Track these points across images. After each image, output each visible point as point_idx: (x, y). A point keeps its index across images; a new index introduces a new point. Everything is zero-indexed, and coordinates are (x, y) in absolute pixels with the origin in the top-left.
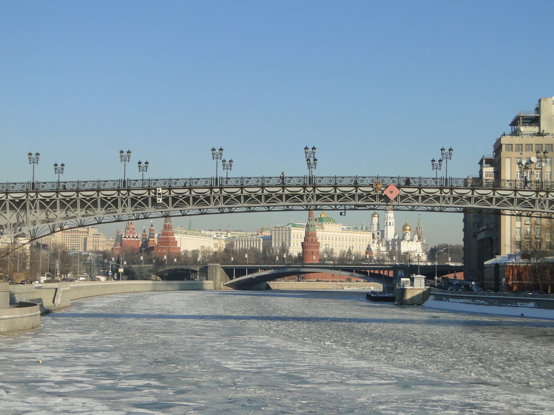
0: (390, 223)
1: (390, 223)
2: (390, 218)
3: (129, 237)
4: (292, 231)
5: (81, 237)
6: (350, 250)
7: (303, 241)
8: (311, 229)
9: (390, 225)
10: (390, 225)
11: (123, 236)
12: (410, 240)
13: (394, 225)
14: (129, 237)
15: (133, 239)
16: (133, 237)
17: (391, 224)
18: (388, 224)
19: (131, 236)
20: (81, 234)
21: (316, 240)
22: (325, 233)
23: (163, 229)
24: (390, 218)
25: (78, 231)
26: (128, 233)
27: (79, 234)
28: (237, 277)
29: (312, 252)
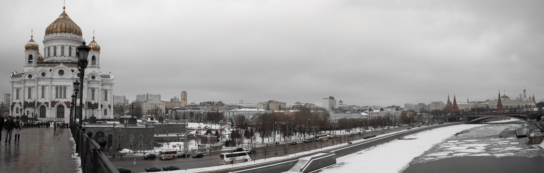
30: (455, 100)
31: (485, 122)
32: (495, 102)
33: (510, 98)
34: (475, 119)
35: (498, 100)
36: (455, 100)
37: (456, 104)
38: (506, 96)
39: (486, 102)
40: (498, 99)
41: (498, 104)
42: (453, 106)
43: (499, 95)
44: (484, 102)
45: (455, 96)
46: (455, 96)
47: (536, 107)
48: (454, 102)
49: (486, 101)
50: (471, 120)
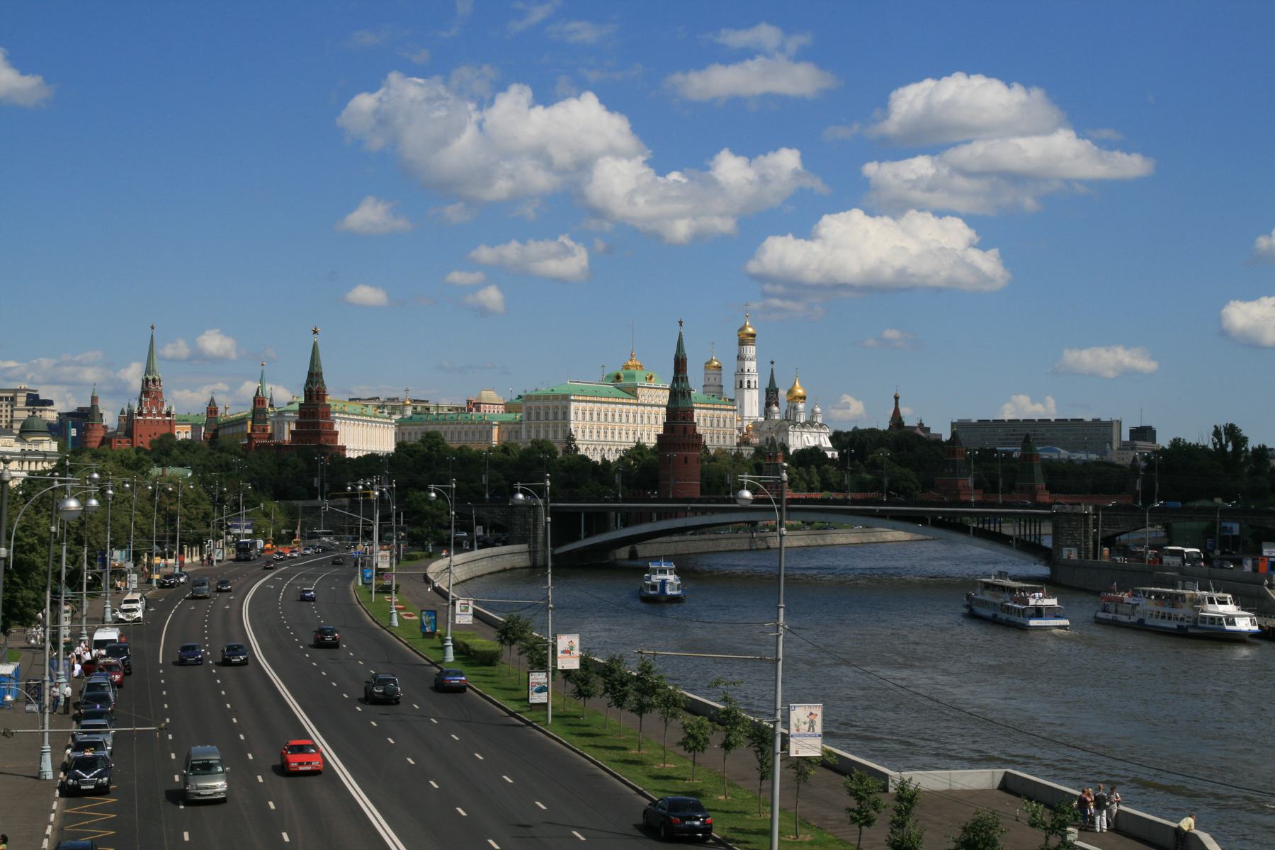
0: (749, 382)
1: (749, 382)
2: (748, 370)
3: (150, 413)
4: (573, 406)
8: (682, 403)
9: (749, 387)
10: (749, 387)
11: (136, 411)
12: (807, 422)
13: (757, 387)
14: (150, 413)
16: (159, 414)
17: (752, 385)
18: (746, 385)
19: (154, 411)
24: (748, 370)
26: (146, 405)
28: (587, 536)
29: (686, 458)
45: (315, 345)
46: (315, 345)
50: (578, 539)
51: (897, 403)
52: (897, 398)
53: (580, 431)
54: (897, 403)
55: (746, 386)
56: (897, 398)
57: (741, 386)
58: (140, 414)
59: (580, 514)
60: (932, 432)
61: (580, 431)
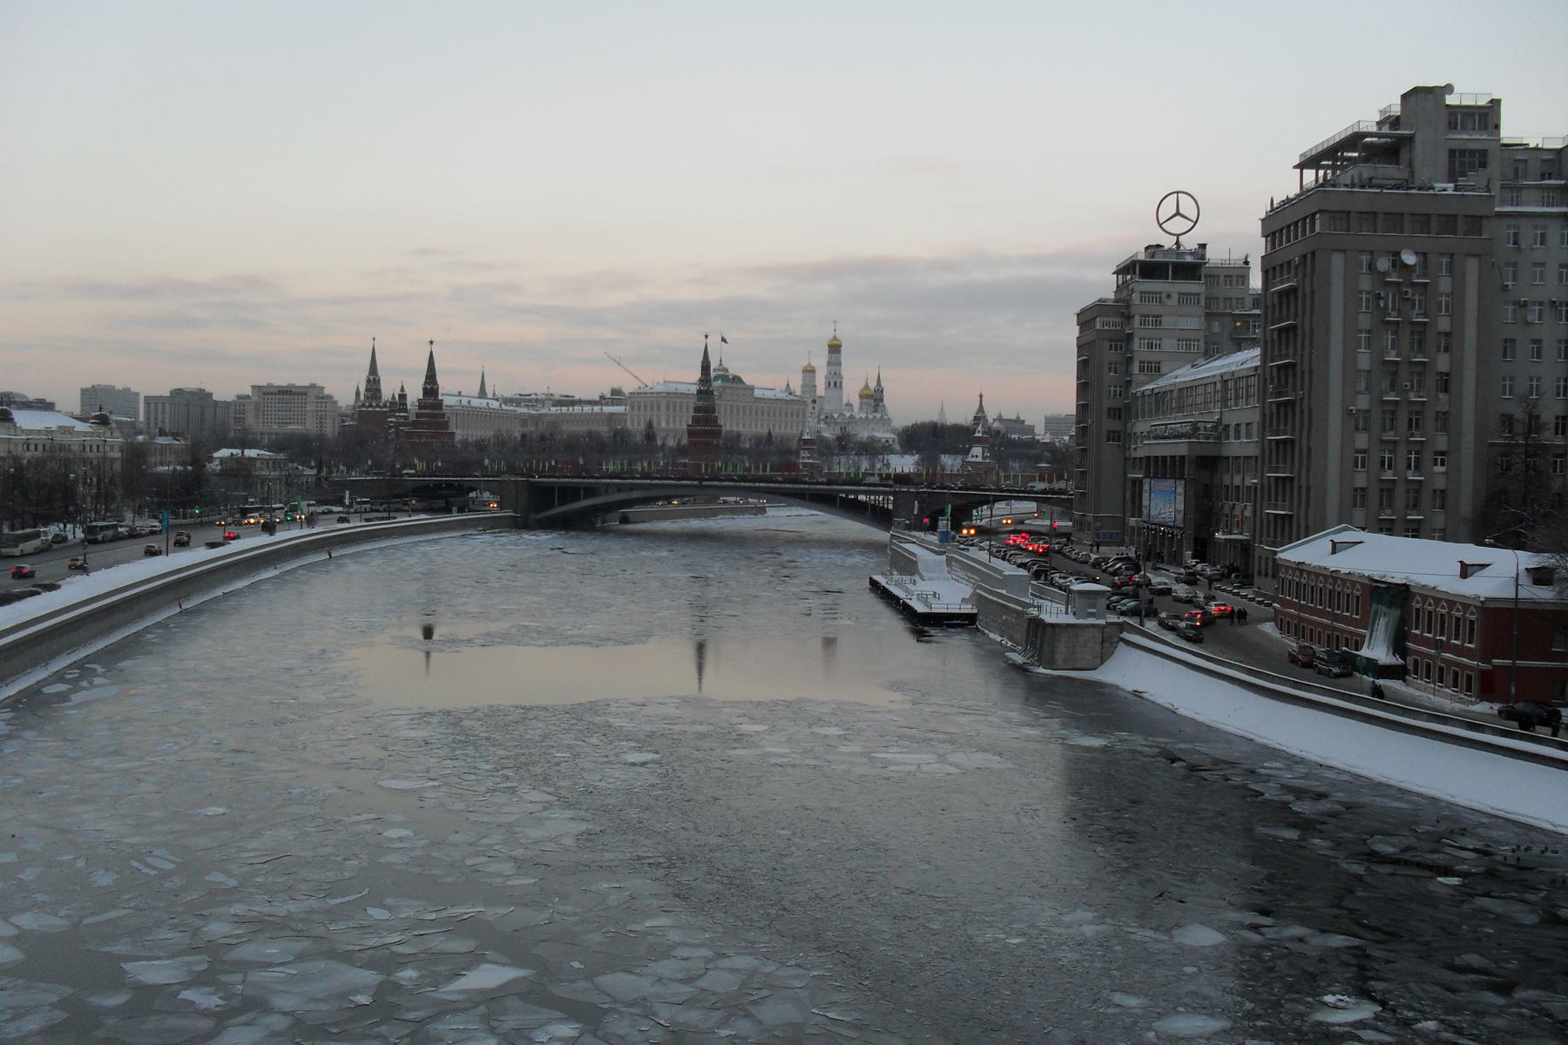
0: (835, 383)
1: (835, 383)
5: (296, 401)
6: (770, 433)
7: (690, 423)
14: (370, 406)
15: (378, 409)
16: (378, 406)
17: (838, 385)
19: (374, 404)
20: (296, 397)
21: (716, 421)
22: (723, 403)
23: (421, 397)
25: (291, 391)
27: (292, 397)
28: (559, 505)
30: (431, 376)
31: (625, 520)
32: (663, 408)
33: (752, 388)
34: (576, 498)
35: (699, 392)
36: (431, 376)
37: (439, 405)
38: (732, 372)
39: (602, 400)
40: (694, 389)
41: (696, 420)
42: (418, 415)
43: (706, 367)
44: (590, 403)
45: (431, 353)
46: (431, 353)
47: (897, 447)
48: (426, 391)
49: (602, 397)
51: (981, 401)
52: (981, 396)
53: (663, 418)
54: (981, 401)
55: (832, 385)
56: (981, 396)
57: (829, 386)
58: (364, 405)
59: (554, 488)
60: (1026, 423)
61: (663, 418)
